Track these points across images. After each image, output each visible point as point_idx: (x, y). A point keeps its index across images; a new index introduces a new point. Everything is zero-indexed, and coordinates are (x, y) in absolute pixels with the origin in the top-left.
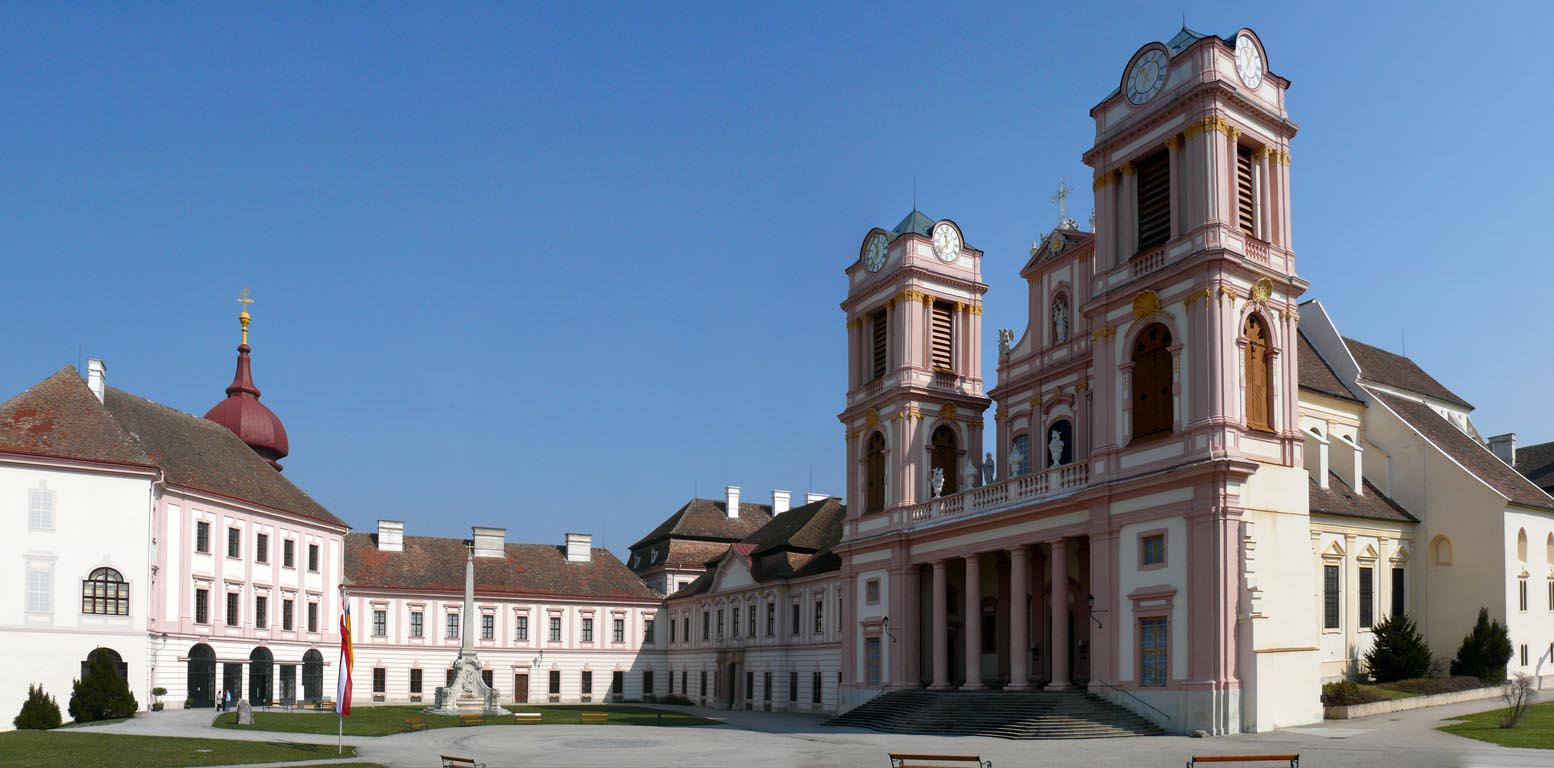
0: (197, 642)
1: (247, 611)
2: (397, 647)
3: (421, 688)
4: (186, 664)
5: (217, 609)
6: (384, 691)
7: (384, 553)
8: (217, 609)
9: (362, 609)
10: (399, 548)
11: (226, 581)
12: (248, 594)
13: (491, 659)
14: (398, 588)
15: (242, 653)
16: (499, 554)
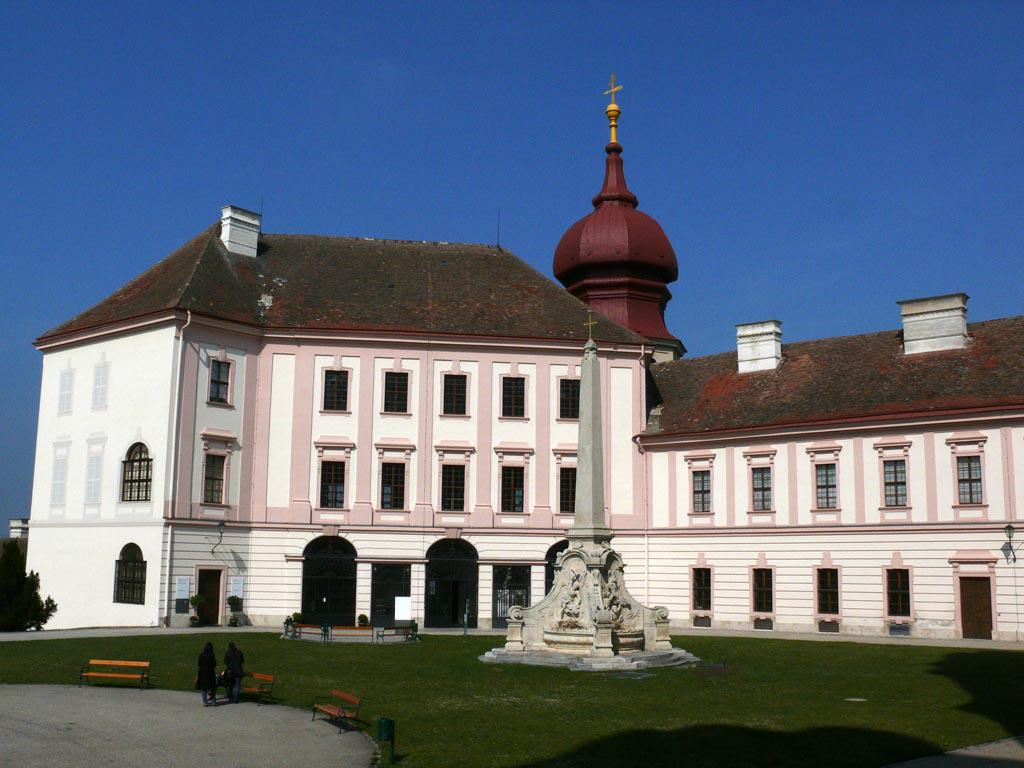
0: (318, 535)
1: (423, 488)
2: (731, 531)
3: (709, 603)
4: (300, 565)
5: (362, 486)
6: (709, 608)
7: (747, 375)
8: (362, 486)
9: (671, 469)
10: (771, 364)
11: (378, 447)
12: (425, 464)
13: (829, 547)
14: (728, 429)
15: (413, 548)
16: (956, 343)
